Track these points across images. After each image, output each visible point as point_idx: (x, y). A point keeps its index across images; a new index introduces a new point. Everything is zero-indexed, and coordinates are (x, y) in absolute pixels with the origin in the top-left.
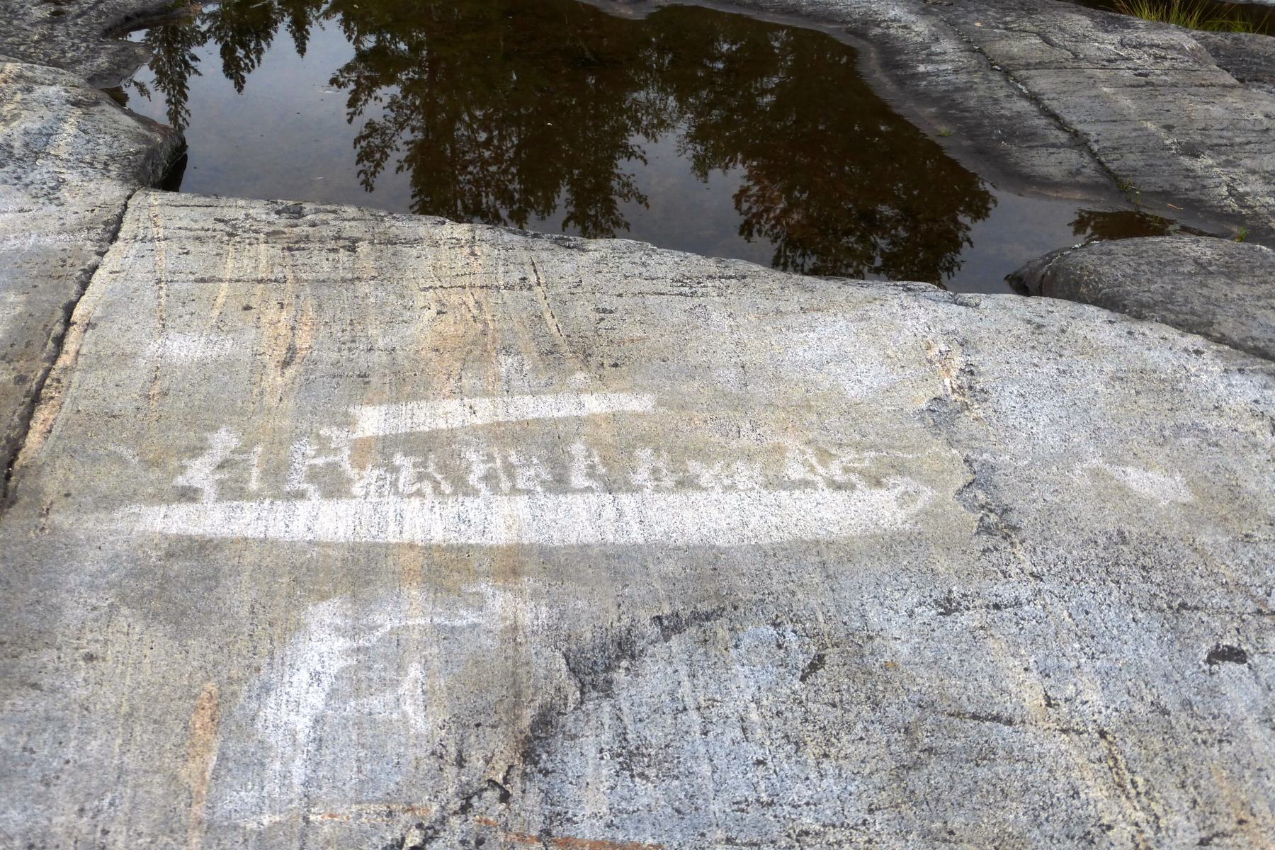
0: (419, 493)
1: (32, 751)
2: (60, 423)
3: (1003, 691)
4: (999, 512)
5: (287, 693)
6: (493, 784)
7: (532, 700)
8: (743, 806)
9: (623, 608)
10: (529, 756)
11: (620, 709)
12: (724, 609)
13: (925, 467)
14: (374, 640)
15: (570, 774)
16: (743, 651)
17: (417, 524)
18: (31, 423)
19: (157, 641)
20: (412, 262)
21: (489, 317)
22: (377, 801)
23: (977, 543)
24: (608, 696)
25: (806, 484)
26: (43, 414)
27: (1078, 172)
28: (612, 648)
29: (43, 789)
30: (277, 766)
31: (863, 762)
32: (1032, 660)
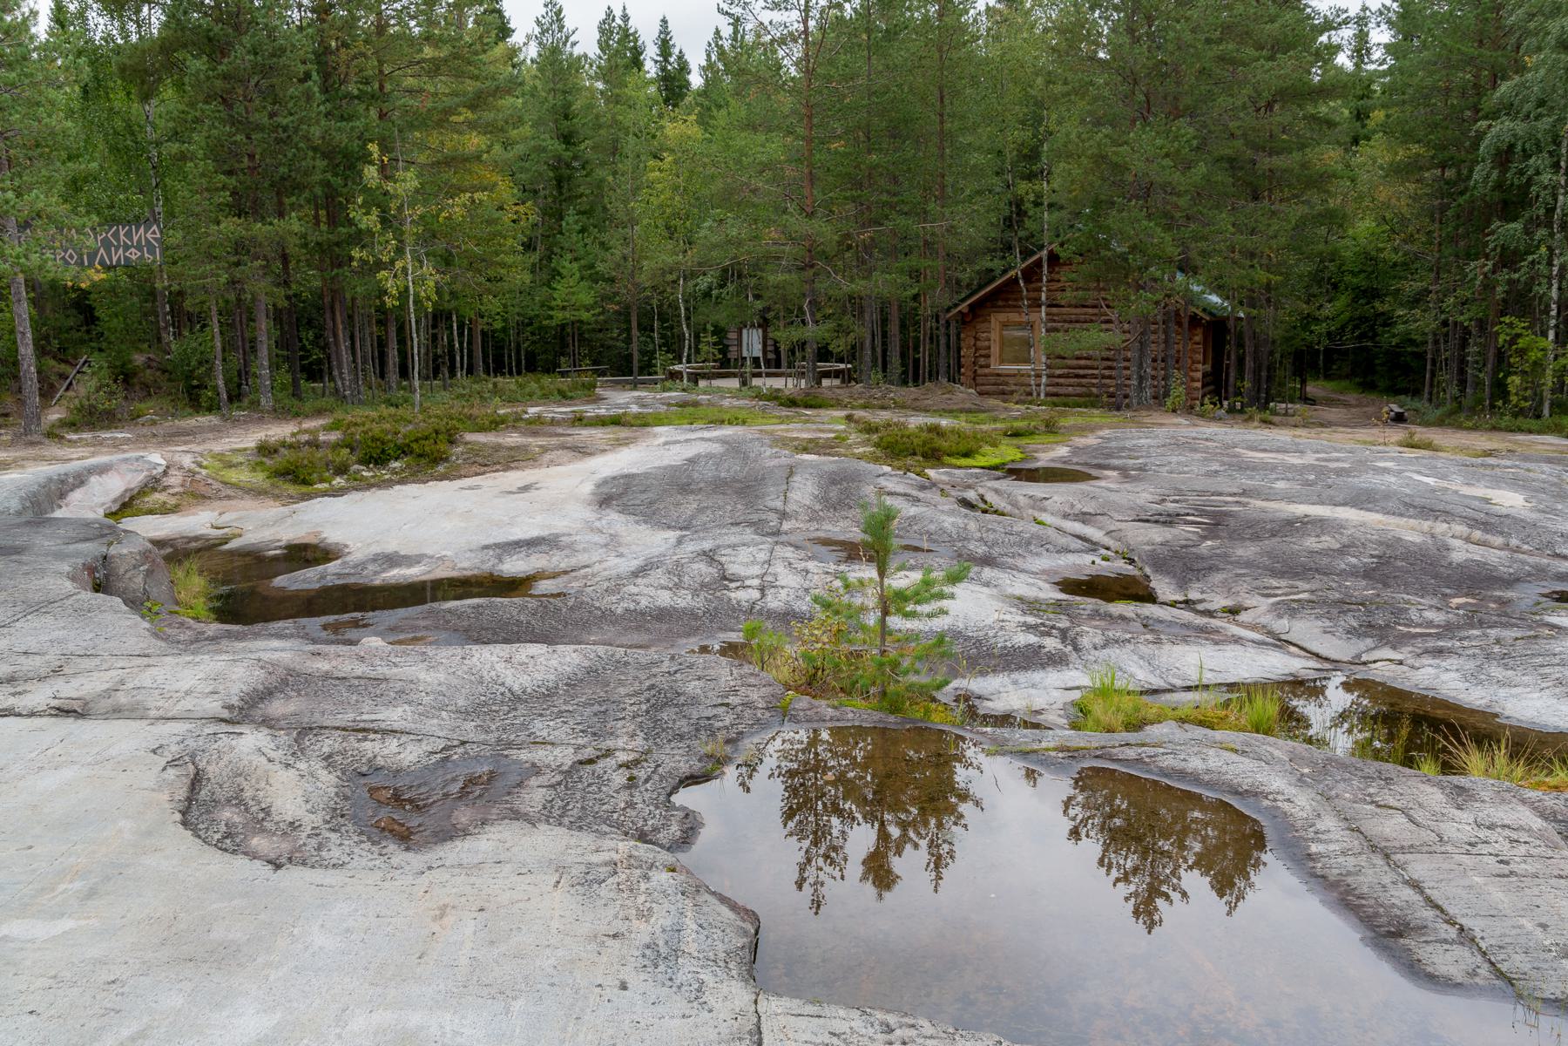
27: (1473, 974)
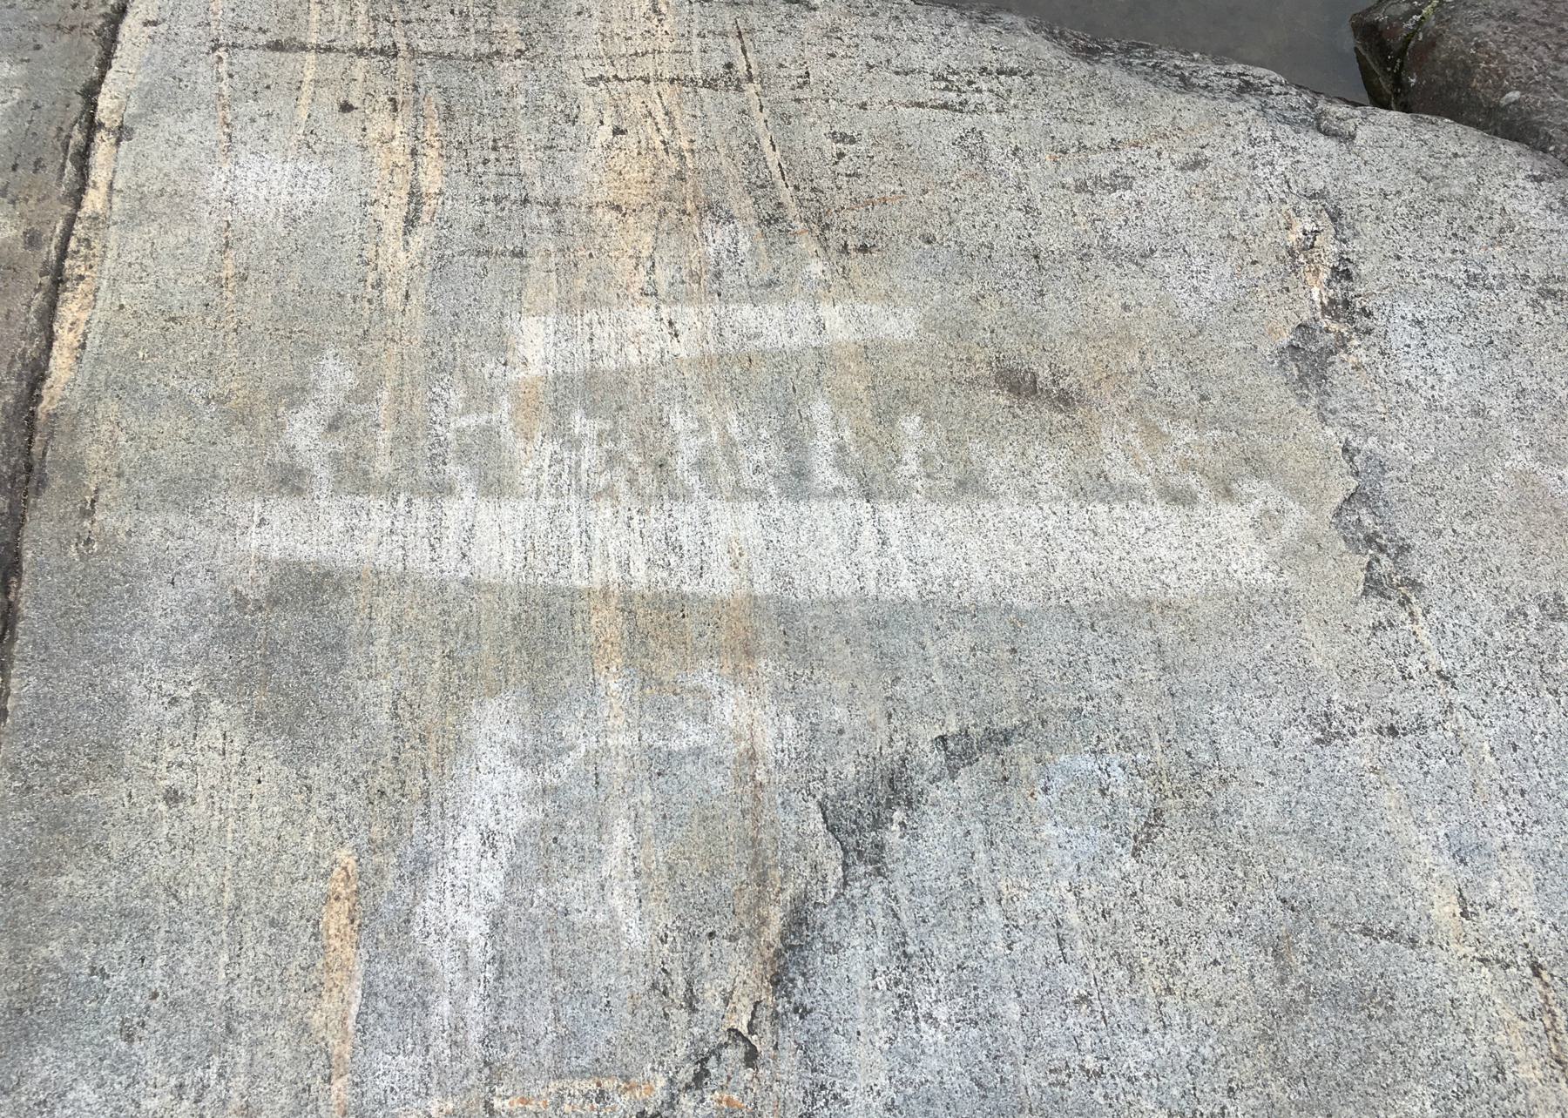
0: (609, 491)
1: (105, 976)
2: (97, 328)
3: (1405, 888)
4: (1392, 551)
5: (452, 871)
6: (734, 1033)
7: (782, 890)
8: (1063, 1077)
9: (895, 722)
10: (778, 982)
11: (896, 899)
12: (1028, 725)
13: (1291, 463)
14: (565, 774)
15: (835, 1016)
16: (1054, 797)
17: (611, 550)
18: (55, 328)
19: (266, 769)
20: (572, 24)
21: (685, 145)
22: (583, 1073)
23: (1365, 613)
24: (878, 872)
25: (1128, 492)
26: (71, 310)
28: (882, 788)
29: (123, 1045)
30: (444, 1007)
31: (1218, 1004)
32: (1441, 833)
